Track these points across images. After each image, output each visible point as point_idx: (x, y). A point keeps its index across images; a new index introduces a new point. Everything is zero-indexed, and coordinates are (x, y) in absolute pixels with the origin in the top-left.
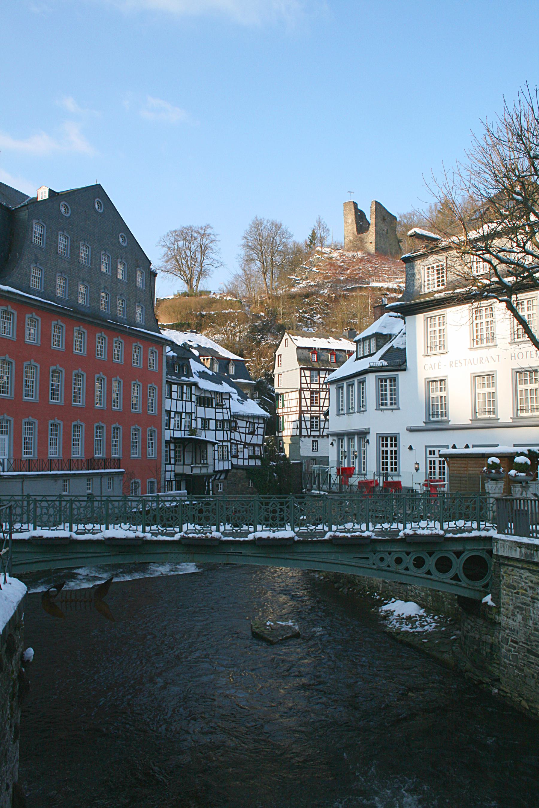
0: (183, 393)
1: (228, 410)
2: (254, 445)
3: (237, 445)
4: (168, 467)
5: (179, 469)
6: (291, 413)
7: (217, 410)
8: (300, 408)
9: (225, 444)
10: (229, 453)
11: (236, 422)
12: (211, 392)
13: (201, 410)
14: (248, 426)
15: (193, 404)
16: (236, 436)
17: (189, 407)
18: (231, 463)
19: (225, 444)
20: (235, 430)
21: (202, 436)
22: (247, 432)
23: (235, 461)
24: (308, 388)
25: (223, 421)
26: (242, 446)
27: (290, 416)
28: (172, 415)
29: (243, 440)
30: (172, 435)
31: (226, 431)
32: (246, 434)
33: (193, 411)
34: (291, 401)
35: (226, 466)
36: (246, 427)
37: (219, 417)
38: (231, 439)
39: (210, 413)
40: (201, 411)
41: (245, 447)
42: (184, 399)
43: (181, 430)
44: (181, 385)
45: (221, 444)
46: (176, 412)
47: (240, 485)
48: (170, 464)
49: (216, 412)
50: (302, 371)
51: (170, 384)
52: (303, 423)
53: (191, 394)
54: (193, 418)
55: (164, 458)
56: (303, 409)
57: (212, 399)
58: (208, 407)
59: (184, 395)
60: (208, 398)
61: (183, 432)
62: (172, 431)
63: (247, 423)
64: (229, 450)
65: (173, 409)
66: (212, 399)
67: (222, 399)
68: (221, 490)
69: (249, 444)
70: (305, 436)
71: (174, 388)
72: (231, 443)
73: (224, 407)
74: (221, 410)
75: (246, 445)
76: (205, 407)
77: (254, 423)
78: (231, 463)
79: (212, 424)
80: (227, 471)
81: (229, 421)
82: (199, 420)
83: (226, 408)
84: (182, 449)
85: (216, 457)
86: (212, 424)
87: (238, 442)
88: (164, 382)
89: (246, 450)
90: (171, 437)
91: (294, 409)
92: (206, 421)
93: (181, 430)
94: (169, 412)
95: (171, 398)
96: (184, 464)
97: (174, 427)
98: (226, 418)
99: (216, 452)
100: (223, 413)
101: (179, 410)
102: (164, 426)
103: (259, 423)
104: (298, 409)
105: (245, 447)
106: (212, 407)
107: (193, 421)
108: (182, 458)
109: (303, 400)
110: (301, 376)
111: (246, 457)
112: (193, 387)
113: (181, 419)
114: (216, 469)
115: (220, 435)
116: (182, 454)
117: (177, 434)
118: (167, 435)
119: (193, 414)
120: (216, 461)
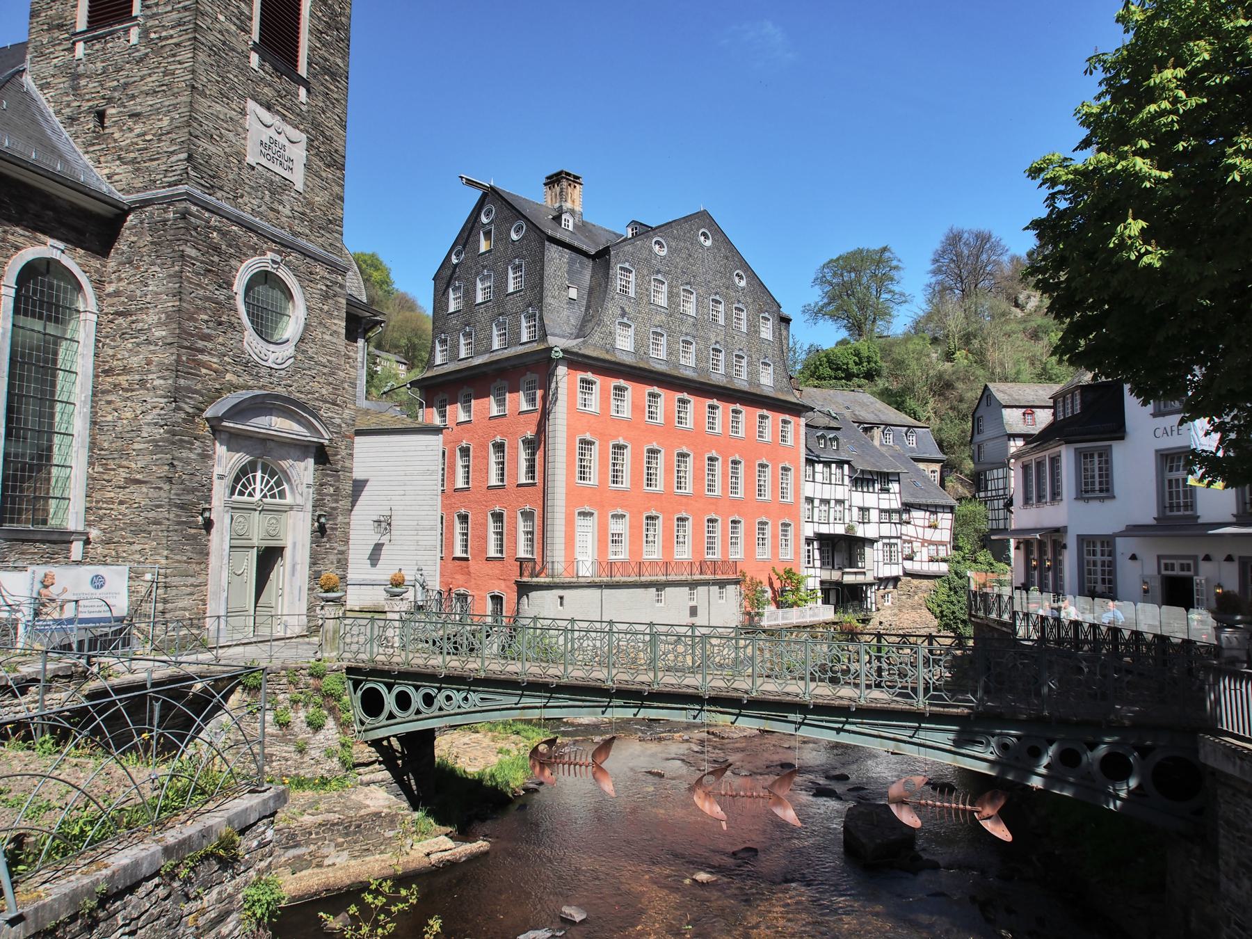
0: (831, 474)
1: (898, 495)
2: (937, 544)
4: (811, 571)
5: (827, 575)
7: (882, 496)
9: (893, 541)
12: (871, 472)
15: (847, 489)
16: (908, 530)
17: (841, 492)
18: (903, 568)
19: (893, 541)
20: (909, 523)
21: (860, 532)
22: (927, 524)
23: (909, 565)
26: (919, 544)
27: (996, 502)
28: (817, 503)
29: (920, 536)
30: (816, 530)
32: (924, 527)
35: (896, 571)
37: (884, 505)
39: (871, 499)
40: (860, 498)
41: (923, 545)
42: (833, 482)
44: (827, 464)
45: (886, 541)
47: (916, 598)
48: (814, 567)
51: (810, 462)
53: (843, 475)
54: (847, 506)
55: (804, 559)
59: (833, 477)
62: (816, 525)
65: (818, 495)
68: (890, 603)
69: (931, 543)
72: (905, 541)
74: (886, 496)
75: (924, 542)
78: (903, 568)
79: (874, 515)
80: (896, 580)
82: (855, 510)
84: (830, 549)
85: (881, 559)
86: (874, 515)
88: (803, 460)
92: (864, 510)
94: (810, 500)
96: (833, 568)
98: (896, 505)
99: (880, 553)
101: (826, 497)
102: (803, 519)
105: (923, 545)
106: (874, 492)
107: (847, 511)
108: (831, 560)
111: (926, 558)
112: (846, 467)
113: (829, 508)
114: (881, 576)
115: (886, 530)
116: (830, 554)
117: (824, 529)
118: (809, 530)
119: (847, 504)
120: (881, 564)
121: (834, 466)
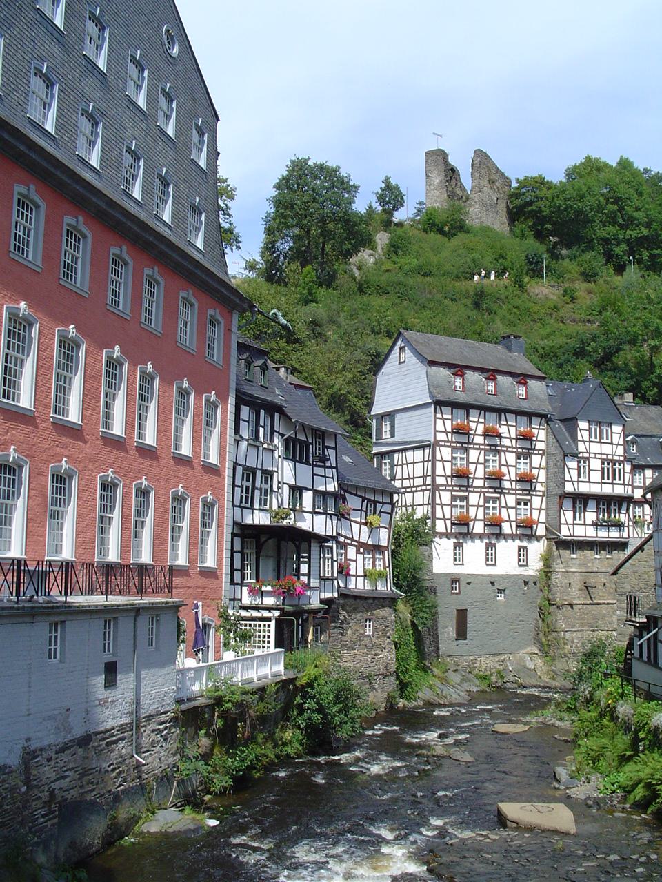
1: (334, 470)
3: (344, 546)
6: (413, 489)
7: (317, 471)
8: (434, 480)
10: (335, 563)
11: (344, 500)
13: (288, 466)
14: (364, 509)
24: (448, 441)
25: (324, 495)
29: (356, 538)
30: (238, 519)
31: (331, 515)
32: (360, 523)
34: (411, 466)
36: (361, 510)
38: (338, 534)
41: (358, 552)
49: (314, 475)
50: (438, 407)
52: (438, 508)
56: (440, 481)
57: (307, 444)
58: (301, 462)
60: (301, 442)
63: (363, 501)
64: (335, 558)
66: (307, 444)
67: (324, 447)
70: (441, 535)
73: (328, 464)
76: (296, 461)
77: (375, 502)
81: (336, 497)
82: (286, 488)
83: (331, 467)
87: (347, 541)
89: (360, 557)
91: (419, 482)
97: (241, 502)
98: (332, 487)
100: (325, 477)
101: (252, 464)
103: (383, 503)
104: (429, 481)
106: (307, 463)
109: (439, 464)
110: (435, 418)
112: (277, 415)
119: (275, 474)
121: (262, 412)
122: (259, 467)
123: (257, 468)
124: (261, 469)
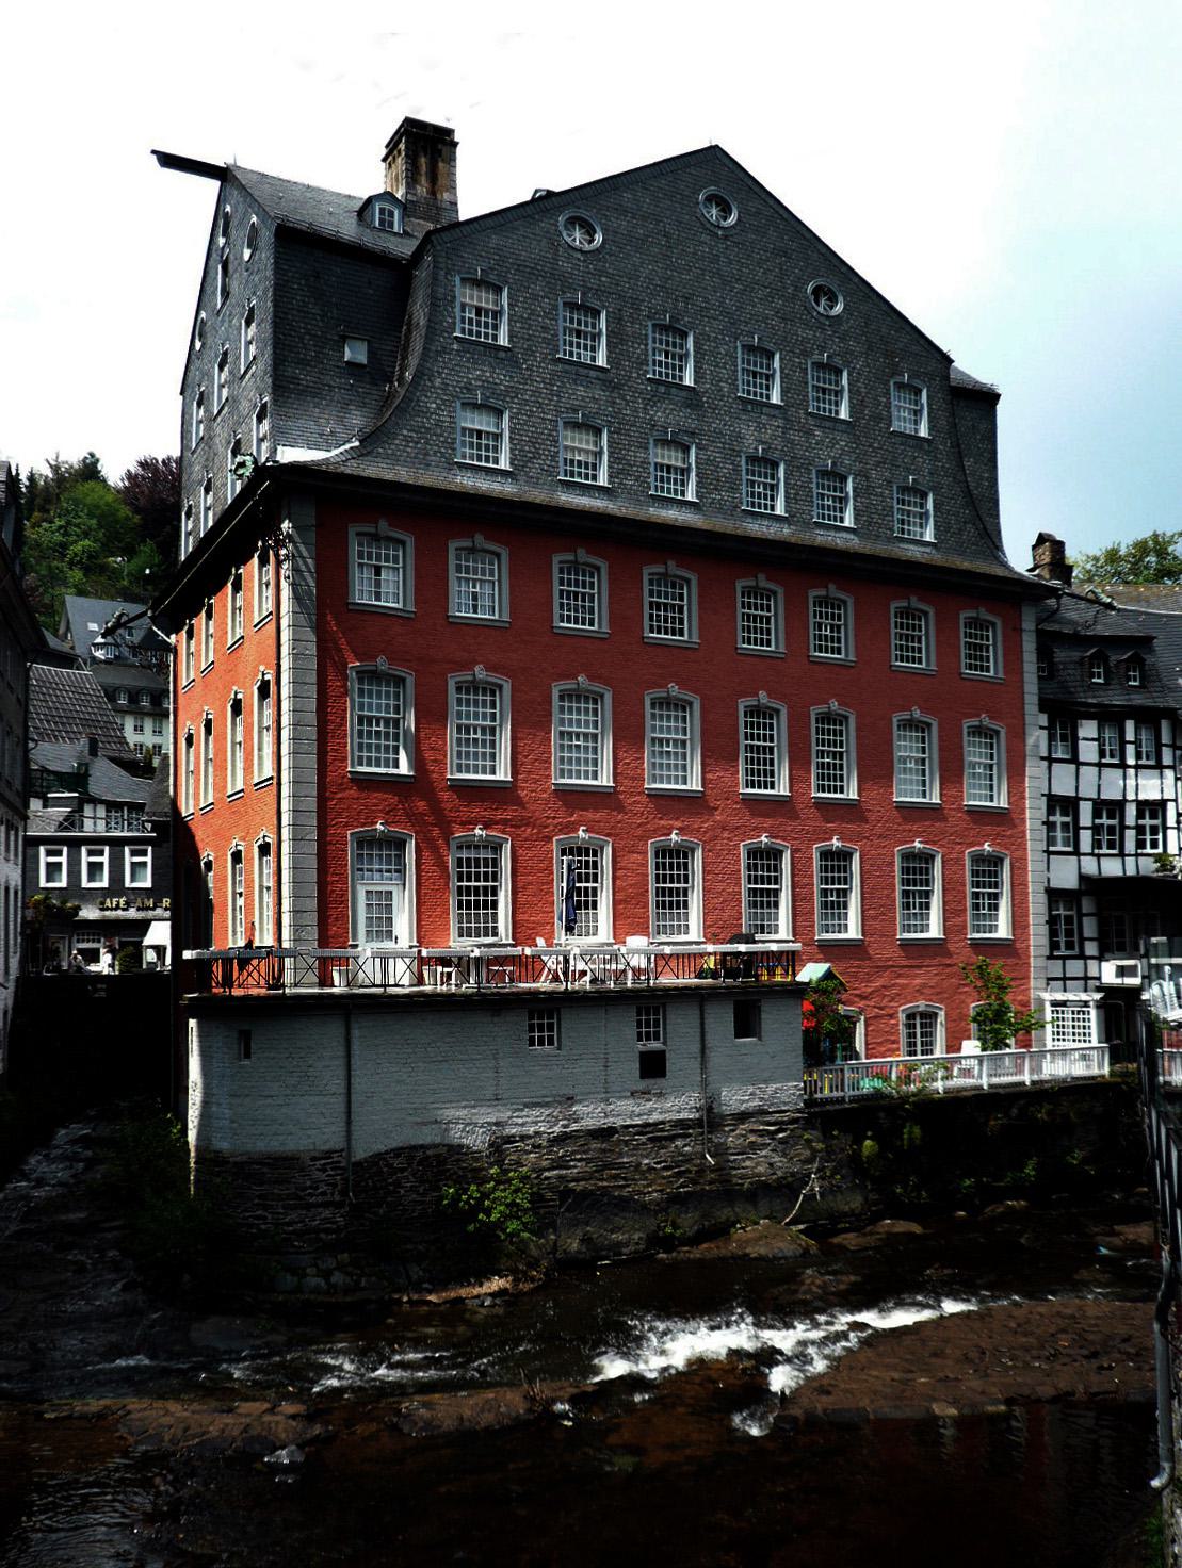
28: (1086, 810)
33: (1169, 794)
42: (1131, 761)
43: (1122, 855)
44: (1111, 718)
46: (1100, 806)
61: (1130, 861)
65: (1088, 790)
71: (1088, 729)
90: (1083, 878)
93: (1122, 855)
95: (1074, 760)
101: (1111, 793)
117: (1112, 868)
118: (1065, 875)
119: (1171, 807)
122: (1131, 796)
123: (1125, 801)
124: (1137, 801)
